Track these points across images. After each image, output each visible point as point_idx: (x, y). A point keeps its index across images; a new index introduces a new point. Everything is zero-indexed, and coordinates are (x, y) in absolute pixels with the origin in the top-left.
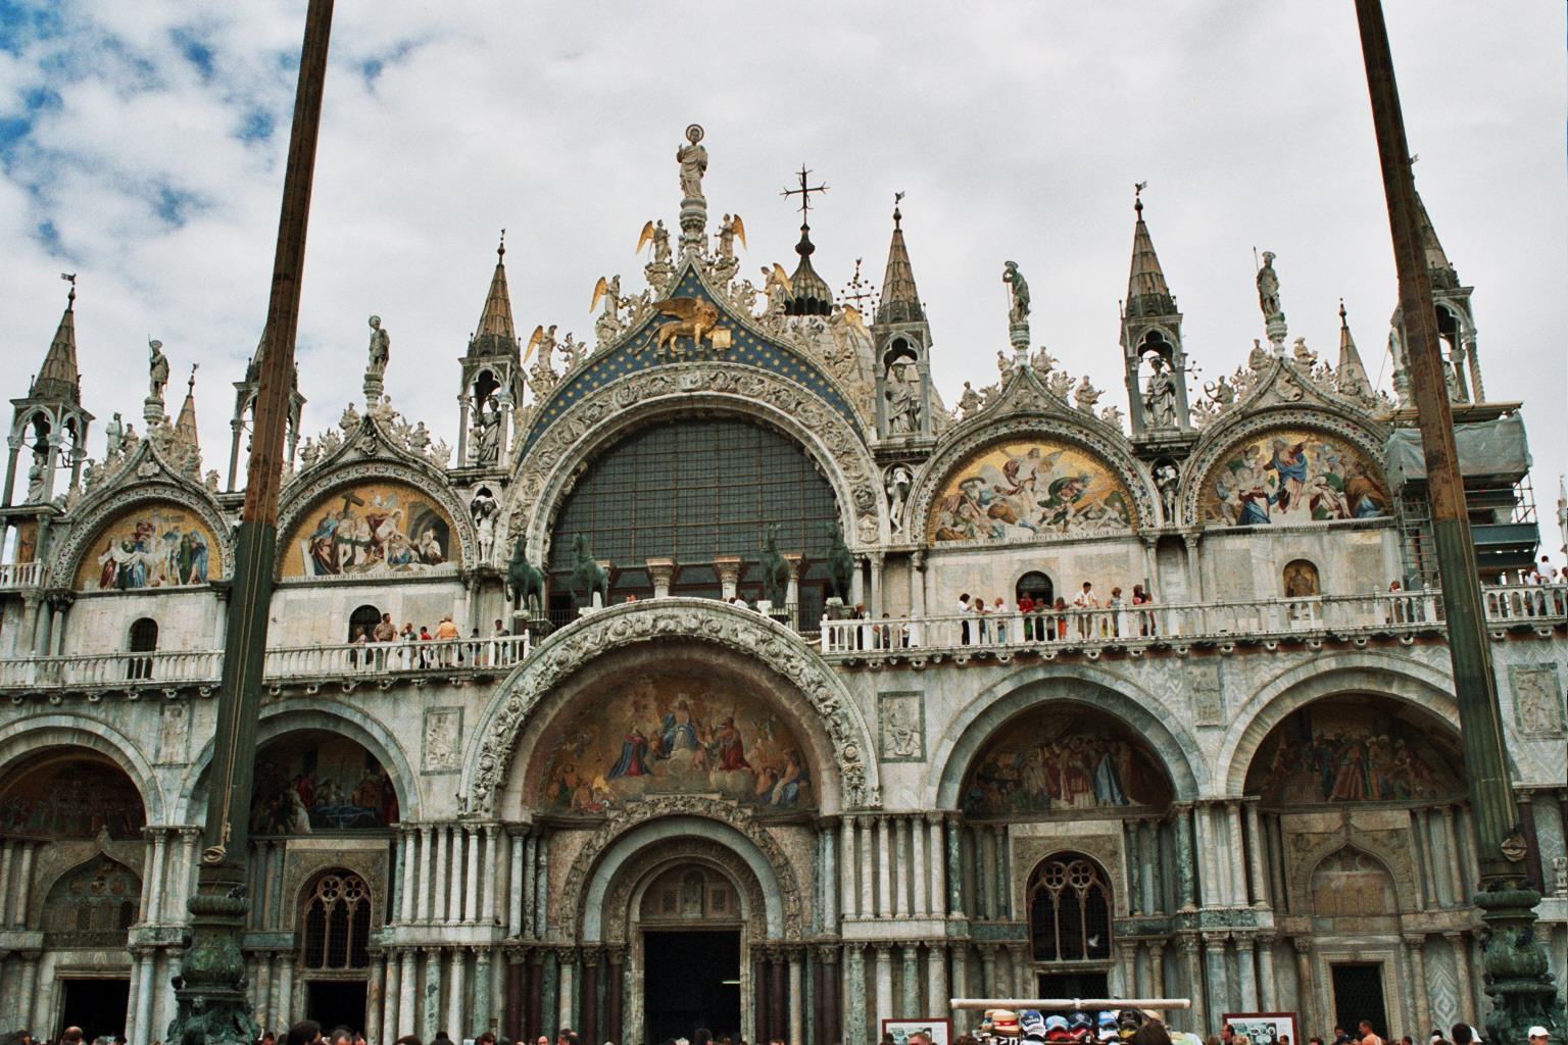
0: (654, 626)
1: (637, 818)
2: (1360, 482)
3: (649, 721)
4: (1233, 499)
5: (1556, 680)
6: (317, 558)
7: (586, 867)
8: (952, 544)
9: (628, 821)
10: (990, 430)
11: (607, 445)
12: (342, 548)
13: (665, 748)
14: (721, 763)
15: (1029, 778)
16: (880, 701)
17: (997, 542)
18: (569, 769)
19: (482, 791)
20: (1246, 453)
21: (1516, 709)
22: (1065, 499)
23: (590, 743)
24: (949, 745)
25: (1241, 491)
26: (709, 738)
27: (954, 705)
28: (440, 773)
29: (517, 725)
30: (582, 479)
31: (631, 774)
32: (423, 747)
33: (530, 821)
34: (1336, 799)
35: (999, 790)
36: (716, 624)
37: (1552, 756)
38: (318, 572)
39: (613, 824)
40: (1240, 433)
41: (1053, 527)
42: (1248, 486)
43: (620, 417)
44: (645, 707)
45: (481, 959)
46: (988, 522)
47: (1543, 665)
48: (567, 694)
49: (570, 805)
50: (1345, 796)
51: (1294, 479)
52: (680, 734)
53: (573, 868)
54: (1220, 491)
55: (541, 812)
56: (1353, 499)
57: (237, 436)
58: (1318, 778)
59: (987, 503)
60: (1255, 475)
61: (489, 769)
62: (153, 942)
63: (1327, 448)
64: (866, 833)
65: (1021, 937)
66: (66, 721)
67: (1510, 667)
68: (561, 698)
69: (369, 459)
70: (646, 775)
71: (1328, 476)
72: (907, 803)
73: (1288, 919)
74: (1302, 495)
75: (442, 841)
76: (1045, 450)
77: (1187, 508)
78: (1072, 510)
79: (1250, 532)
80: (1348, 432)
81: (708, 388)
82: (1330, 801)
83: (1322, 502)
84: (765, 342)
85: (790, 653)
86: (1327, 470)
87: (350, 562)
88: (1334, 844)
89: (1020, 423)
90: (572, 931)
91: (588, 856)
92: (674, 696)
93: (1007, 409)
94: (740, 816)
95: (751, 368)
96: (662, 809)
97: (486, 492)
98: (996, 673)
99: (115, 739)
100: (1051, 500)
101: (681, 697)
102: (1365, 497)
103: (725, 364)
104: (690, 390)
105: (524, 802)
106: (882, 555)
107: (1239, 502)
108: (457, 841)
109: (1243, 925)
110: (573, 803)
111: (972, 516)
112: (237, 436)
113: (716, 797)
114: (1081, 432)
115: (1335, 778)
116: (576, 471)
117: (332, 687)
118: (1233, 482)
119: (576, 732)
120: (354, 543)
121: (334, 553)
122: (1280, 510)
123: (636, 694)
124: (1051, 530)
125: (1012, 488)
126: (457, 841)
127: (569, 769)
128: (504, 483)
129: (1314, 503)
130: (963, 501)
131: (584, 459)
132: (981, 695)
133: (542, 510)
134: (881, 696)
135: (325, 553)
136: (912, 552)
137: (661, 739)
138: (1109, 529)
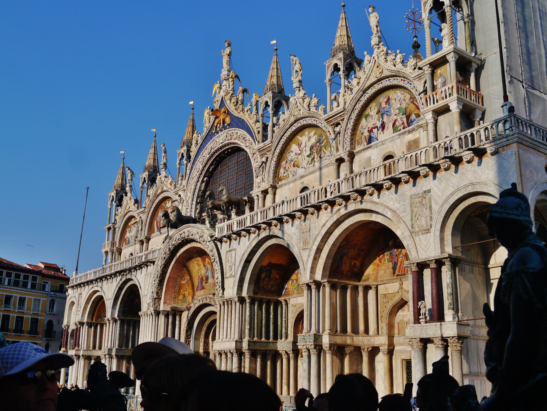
1: (197, 306)
2: (412, 107)
4: (366, 134)
5: (430, 200)
6: (157, 226)
8: (283, 182)
10: (290, 130)
11: (211, 169)
13: (207, 278)
15: (300, 278)
17: (295, 177)
18: (185, 290)
20: (370, 108)
21: (412, 219)
22: (314, 151)
25: (369, 128)
30: (207, 184)
33: (168, 309)
34: (398, 275)
35: (292, 284)
37: (425, 243)
40: (364, 99)
41: (310, 165)
42: (371, 125)
46: (293, 169)
47: (425, 192)
50: (400, 273)
51: (387, 115)
54: (362, 130)
55: (175, 305)
56: (408, 117)
58: (391, 265)
59: (292, 161)
60: (373, 118)
61: (152, 293)
63: (399, 94)
65: (290, 348)
67: (411, 197)
70: (204, 289)
71: (399, 109)
72: (230, 294)
73: (376, 338)
74: (390, 122)
75: (146, 317)
76: (306, 132)
77: (346, 143)
78: (316, 156)
79: (370, 147)
80: (401, 83)
82: (395, 277)
83: (397, 123)
86: (399, 106)
88: (397, 299)
89: (298, 123)
92: (205, 259)
93: (292, 119)
95: (234, 129)
96: (201, 303)
97: (180, 196)
100: (310, 153)
102: (413, 115)
103: (228, 130)
104: (222, 143)
105: (164, 303)
106: (260, 192)
107: (368, 134)
108: (148, 317)
109: (310, 342)
110: (187, 302)
111: (289, 168)
114: (315, 120)
115: (397, 263)
116: (203, 181)
117: (130, 270)
118: (366, 124)
122: (382, 133)
124: (309, 167)
125: (299, 152)
126: (148, 317)
127: (185, 290)
129: (394, 124)
130: (287, 163)
132: (248, 247)
135: (158, 225)
136: (267, 189)
138: (326, 161)
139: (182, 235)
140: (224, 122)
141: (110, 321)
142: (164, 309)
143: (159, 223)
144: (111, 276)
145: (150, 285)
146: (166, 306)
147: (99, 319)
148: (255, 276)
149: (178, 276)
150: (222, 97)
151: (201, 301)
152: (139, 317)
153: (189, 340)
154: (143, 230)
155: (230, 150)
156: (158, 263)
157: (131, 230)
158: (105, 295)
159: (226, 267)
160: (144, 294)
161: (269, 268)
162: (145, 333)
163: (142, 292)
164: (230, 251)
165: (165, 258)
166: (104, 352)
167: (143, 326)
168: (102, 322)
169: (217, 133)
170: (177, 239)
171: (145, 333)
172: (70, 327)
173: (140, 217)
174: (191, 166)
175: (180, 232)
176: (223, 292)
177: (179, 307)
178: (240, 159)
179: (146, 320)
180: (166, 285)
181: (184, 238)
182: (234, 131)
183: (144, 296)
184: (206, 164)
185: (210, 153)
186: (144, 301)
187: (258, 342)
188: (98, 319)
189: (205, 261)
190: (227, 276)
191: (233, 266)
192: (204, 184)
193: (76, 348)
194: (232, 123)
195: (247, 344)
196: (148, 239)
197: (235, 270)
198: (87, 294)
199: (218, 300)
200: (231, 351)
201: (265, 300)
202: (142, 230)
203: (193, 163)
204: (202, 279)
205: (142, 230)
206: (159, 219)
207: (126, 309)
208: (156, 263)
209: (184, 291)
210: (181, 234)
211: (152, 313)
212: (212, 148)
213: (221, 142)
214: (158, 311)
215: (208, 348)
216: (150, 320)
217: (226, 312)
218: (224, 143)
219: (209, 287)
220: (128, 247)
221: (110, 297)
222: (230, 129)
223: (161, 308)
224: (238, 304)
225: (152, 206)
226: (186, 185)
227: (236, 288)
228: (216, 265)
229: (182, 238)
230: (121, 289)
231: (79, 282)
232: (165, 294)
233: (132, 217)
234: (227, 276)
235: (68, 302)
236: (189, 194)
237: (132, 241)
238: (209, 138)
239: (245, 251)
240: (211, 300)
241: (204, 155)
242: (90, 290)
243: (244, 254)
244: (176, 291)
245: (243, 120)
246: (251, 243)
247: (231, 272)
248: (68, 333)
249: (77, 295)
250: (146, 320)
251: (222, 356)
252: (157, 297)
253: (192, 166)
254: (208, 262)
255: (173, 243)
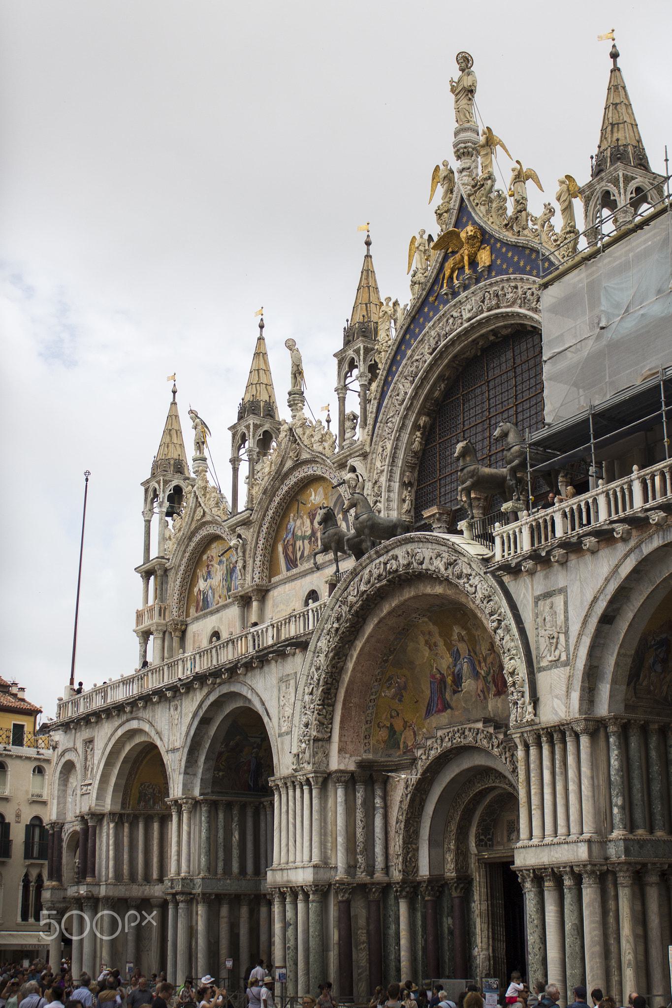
0: (385, 568)
3: (442, 657)
6: (286, 556)
7: (405, 806)
9: (427, 759)
11: (437, 394)
12: (299, 543)
13: (458, 680)
14: (494, 689)
16: (536, 603)
18: (394, 713)
19: (304, 745)
23: (405, 688)
24: (586, 641)
26: (483, 664)
27: (589, 598)
28: (287, 733)
29: (321, 683)
30: (429, 434)
31: (439, 711)
32: (279, 712)
33: (352, 767)
36: (419, 557)
38: (288, 570)
39: (420, 762)
43: (432, 366)
44: (435, 645)
45: (311, 897)
48: (359, 644)
49: (399, 748)
52: (465, 666)
53: (400, 807)
55: (370, 756)
57: (235, 471)
62: (170, 891)
64: (533, 751)
66: (134, 724)
68: (355, 650)
69: (298, 464)
70: (449, 711)
72: (556, 713)
75: (291, 792)
81: (482, 312)
84: (515, 247)
85: (469, 571)
87: (302, 556)
90: (400, 867)
91: (407, 795)
92: (452, 629)
94: (496, 744)
95: (505, 277)
96: (447, 744)
97: (353, 470)
98: (621, 549)
99: (153, 733)
101: (456, 630)
104: (470, 319)
105: (341, 750)
110: (401, 746)
112: (235, 471)
113: (480, 725)
116: (416, 427)
117: (233, 671)
119: (390, 678)
120: (303, 538)
121: (294, 552)
123: (423, 633)
127: (394, 713)
128: (365, 456)
131: (419, 415)
132: (607, 580)
133: (391, 471)
134: (537, 599)
137: (453, 673)
139: (388, 566)
140: (473, 263)
141: (181, 806)
142: (342, 767)
143: (290, 548)
144: (174, 689)
145: (299, 704)
146: (347, 760)
147: (142, 804)
148: (629, 660)
149: (374, 679)
150: (462, 200)
151: (447, 739)
152: (268, 792)
153: (414, 846)
154: (249, 568)
155: (492, 338)
156: (319, 644)
157: (209, 573)
158: (161, 739)
159: (537, 642)
160: (280, 729)
161: (664, 636)
162: (291, 834)
163: (273, 727)
164: (548, 595)
165: (337, 630)
166: (172, 888)
167: (284, 816)
168: (150, 812)
169: (455, 294)
170: (375, 576)
171: (291, 834)
172: (66, 827)
173: (239, 536)
174: (380, 390)
175: (382, 559)
176: (535, 708)
177: (383, 760)
178: (524, 358)
179: (291, 798)
180: (344, 704)
181: (397, 571)
182: (506, 285)
183: (280, 735)
184: (424, 380)
185: (434, 350)
186: (283, 749)
187: (650, 841)
188: (139, 803)
189: (452, 635)
190: (544, 663)
191: (562, 637)
192: (418, 434)
193: (89, 879)
194: (499, 262)
195: (622, 848)
196: (263, 593)
197: (567, 645)
198: (110, 739)
199: (519, 730)
200: (576, 869)
201: (656, 726)
202: (244, 567)
203: (386, 383)
204: (443, 681)
205: (244, 567)
206: (290, 536)
207: (221, 774)
208: (311, 647)
209: (392, 717)
210: (385, 564)
211: (308, 779)
212: (439, 335)
213: (466, 315)
214: (325, 772)
215: (467, 866)
216: (302, 797)
217: (546, 763)
218: (478, 318)
219: (466, 701)
220: (205, 616)
221: (178, 744)
222: (493, 280)
223: (335, 764)
224: (584, 740)
225: (270, 504)
226: (369, 441)
227: (575, 696)
228: (507, 638)
229: (390, 573)
230: (205, 721)
231: (82, 710)
232: (342, 728)
233: (216, 538)
234: (544, 663)
235: (57, 764)
236: (378, 464)
237: (215, 601)
238: (429, 311)
239: (601, 591)
240: (479, 737)
241: (416, 357)
242: (116, 730)
243: (595, 600)
244: (369, 719)
245: (533, 250)
246: (617, 566)
247: (557, 653)
248: (61, 840)
249: (80, 746)
250: (291, 798)
251: (546, 884)
252: (320, 736)
253: (383, 388)
254: (459, 634)
255: (363, 588)
